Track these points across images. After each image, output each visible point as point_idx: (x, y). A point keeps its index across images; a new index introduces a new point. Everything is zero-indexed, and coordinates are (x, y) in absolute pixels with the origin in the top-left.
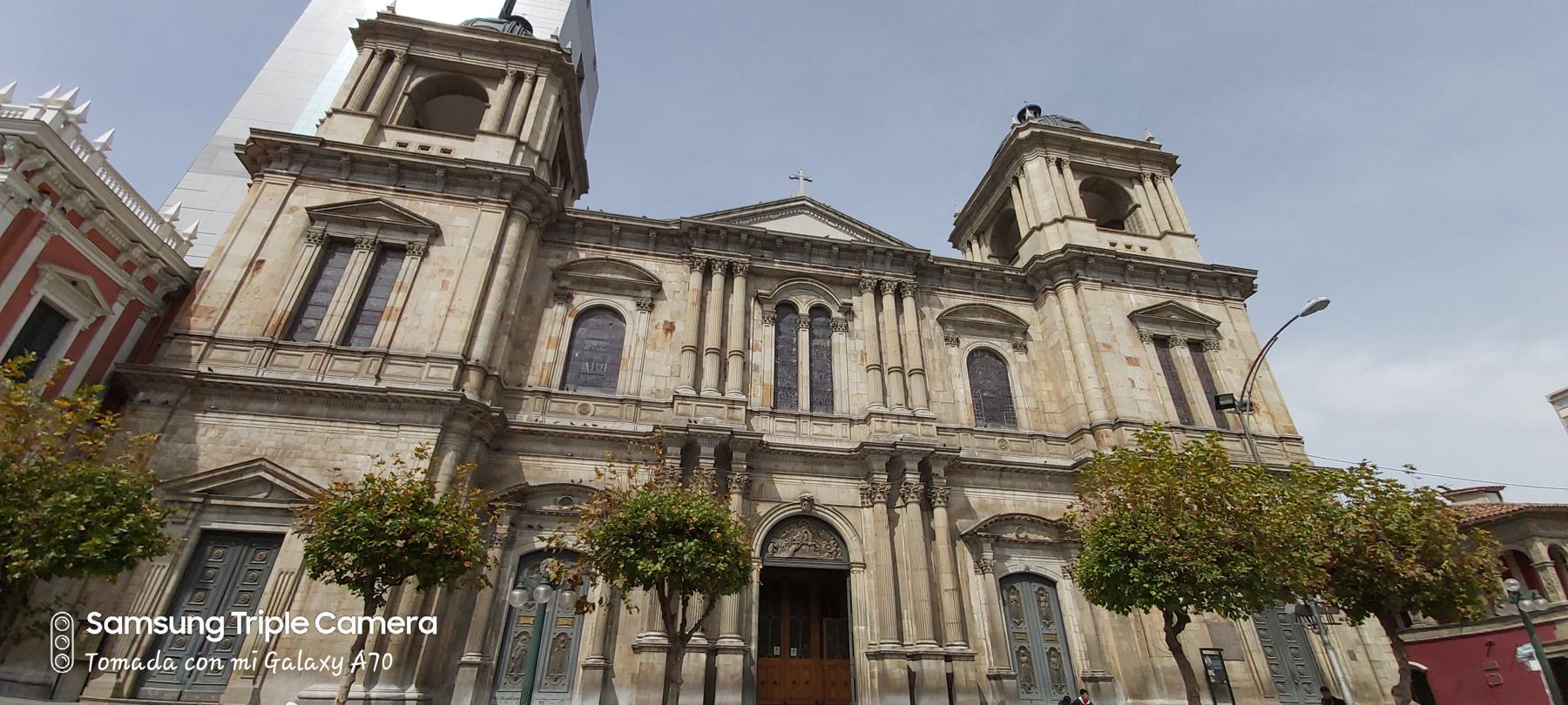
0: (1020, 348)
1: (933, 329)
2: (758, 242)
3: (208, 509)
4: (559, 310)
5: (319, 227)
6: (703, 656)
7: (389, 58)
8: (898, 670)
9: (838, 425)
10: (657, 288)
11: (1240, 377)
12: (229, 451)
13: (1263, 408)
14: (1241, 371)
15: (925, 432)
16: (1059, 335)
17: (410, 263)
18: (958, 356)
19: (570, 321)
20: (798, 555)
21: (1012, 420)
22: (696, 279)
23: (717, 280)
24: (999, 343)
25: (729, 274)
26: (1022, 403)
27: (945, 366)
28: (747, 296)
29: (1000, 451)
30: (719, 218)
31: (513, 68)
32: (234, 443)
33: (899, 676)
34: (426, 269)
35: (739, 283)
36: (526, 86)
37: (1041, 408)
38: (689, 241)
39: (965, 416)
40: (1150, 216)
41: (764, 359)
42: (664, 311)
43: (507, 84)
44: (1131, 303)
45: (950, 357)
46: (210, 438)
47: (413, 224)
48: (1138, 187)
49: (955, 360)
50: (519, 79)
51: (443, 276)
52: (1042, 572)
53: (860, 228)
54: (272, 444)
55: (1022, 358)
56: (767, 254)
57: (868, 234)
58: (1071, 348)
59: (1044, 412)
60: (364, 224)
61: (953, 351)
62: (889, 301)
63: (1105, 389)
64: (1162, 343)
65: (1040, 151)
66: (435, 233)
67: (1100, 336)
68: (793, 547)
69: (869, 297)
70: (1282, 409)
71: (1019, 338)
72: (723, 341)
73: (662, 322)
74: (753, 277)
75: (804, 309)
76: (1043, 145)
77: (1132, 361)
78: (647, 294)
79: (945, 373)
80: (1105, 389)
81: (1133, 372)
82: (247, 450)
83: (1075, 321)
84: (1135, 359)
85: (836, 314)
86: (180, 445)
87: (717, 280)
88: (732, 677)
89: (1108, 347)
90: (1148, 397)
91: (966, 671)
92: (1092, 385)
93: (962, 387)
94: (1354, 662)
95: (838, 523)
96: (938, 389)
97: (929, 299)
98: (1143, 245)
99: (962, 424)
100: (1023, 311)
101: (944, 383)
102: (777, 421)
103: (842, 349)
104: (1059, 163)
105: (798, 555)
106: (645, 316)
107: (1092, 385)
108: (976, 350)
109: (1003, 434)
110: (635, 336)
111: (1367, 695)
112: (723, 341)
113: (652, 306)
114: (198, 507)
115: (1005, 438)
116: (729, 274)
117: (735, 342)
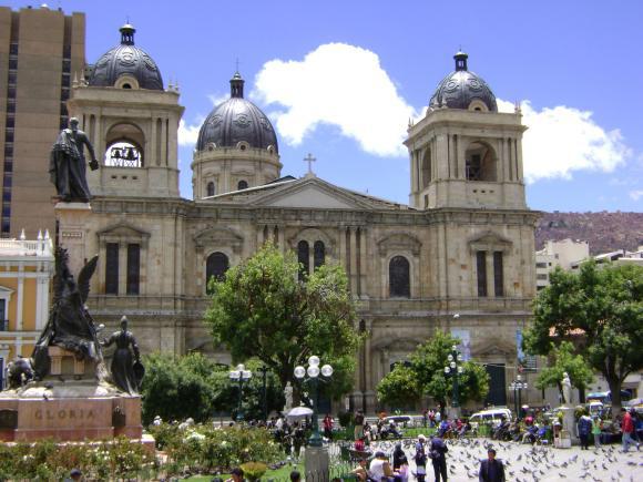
0: (417, 254)
4: (200, 257)
5: (102, 238)
10: (240, 239)
16: (433, 252)
17: (143, 253)
18: (385, 262)
19: (205, 263)
21: (408, 294)
22: (260, 236)
23: (271, 236)
25: (276, 230)
26: (413, 284)
31: (155, 117)
34: (150, 255)
35: (281, 237)
39: (385, 292)
45: (380, 263)
47: (140, 233)
50: (159, 120)
51: (157, 258)
55: (417, 261)
56: (293, 217)
58: (438, 258)
60: (119, 235)
61: (383, 260)
62: (353, 238)
63: (447, 282)
64: (481, 256)
65: (445, 130)
66: (149, 235)
67: (451, 255)
69: (343, 236)
71: (417, 249)
75: (311, 245)
76: (447, 126)
77: (464, 267)
78: (238, 244)
80: (447, 282)
81: (464, 274)
83: (441, 245)
85: (328, 245)
89: (453, 260)
92: (443, 279)
93: (385, 279)
106: (238, 258)
107: (443, 279)
116: (276, 230)
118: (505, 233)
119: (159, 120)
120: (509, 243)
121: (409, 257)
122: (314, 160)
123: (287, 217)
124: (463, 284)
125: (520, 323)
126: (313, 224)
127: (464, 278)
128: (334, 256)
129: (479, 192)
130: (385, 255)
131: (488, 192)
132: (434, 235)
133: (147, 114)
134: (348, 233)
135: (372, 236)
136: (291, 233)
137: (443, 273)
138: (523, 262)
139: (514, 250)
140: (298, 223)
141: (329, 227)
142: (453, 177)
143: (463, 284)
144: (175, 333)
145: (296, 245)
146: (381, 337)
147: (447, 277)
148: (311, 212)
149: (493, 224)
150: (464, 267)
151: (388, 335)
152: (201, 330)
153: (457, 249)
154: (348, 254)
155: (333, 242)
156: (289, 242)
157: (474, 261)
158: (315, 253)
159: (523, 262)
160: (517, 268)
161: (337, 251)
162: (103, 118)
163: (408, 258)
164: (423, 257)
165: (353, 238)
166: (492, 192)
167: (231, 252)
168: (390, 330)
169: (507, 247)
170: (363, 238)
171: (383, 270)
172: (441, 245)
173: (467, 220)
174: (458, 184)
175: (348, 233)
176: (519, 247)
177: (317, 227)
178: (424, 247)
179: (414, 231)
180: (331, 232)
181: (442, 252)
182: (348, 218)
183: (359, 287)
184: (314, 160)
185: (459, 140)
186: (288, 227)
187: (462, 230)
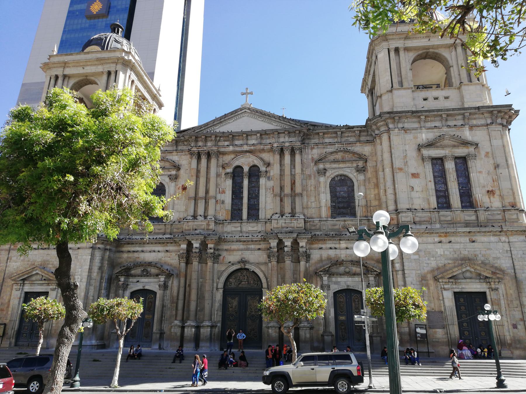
1: (312, 169)
2: (221, 138)
3: (25, 285)
6: (194, 329)
7: (57, 77)
8: (274, 334)
9: (260, 225)
10: (178, 168)
11: (487, 175)
12: (28, 264)
13: (497, 193)
14: (489, 171)
15: (298, 226)
18: (324, 182)
20: (240, 286)
22: (194, 162)
23: (204, 161)
24: (349, 171)
25: (209, 155)
27: (317, 188)
28: (217, 166)
29: (342, 230)
30: (204, 128)
32: (29, 261)
33: (274, 336)
35: (213, 161)
36: (113, 77)
37: (369, 204)
38: (190, 143)
39: (325, 212)
40: (456, 73)
41: (228, 197)
42: (181, 182)
43: (105, 77)
44: (423, 140)
45: (320, 183)
46: (22, 260)
48: (454, 53)
49: (322, 185)
50: (109, 73)
52: (356, 289)
53: (274, 119)
54: (40, 260)
55: (361, 177)
56: (226, 143)
57: (278, 122)
58: (383, 170)
59: (371, 206)
61: (322, 179)
62: (287, 158)
63: (395, 194)
65: (385, 44)
67: (398, 164)
68: (239, 282)
69: (277, 157)
70: (511, 191)
72: (207, 192)
73: (181, 186)
74: (221, 156)
75: (246, 169)
76: (387, 40)
77: (415, 176)
78: (174, 172)
79: (317, 192)
80: (395, 194)
81: (415, 182)
82: (33, 263)
84: (417, 174)
85: (263, 169)
86: (14, 263)
87: (204, 161)
88: (206, 337)
89: (400, 169)
90: (420, 196)
91: (305, 334)
92: (390, 191)
93: (325, 198)
94: (515, 329)
95: (257, 271)
96: (312, 201)
97: (312, 151)
98: (446, 95)
99: (323, 218)
100: (366, 150)
101: (315, 197)
102: (232, 226)
103: (264, 187)
104: (397, 50)
105: (240, 286)
106: (173, 184)
108: (337, 176)
109: (345, 221)
110: (169, 195)
111: (518, 346)
112: (207, 192)
113: (176, 178)
114: (22, 285)
115: (346, 223)
116: (209, 155)
117: (212, 193)
118: (467, 134)
119: (109, 73)
120: (476, 145)
121: (352, 174)
122: (251, 93)
123: (220, 144)
124: (414, 194)
125: (503, 238)
126: (246, 148)
127: (416, 188)
128: (269, 178)
129: (431, 99)
130: (325, 173)
131: (441, 98)
132: (379, 147)
133: (100, 69)
134: (282, 151)
135: (310, 157)
136: (227, 158)
137: (389, 183)
138: (497, 167)
139: (483, 153)
140: (231, 148)
141: (263, 150)
142: (396, 85)
143: (414, 194)
144: (93, 255)
145: (230, 170)
146: (321, 260)
147: (395, 189)
148: (248, 134)
149: (449, 126)
150: (415, 176)
151: (329, 258)
152: (130, 255)
153: (406, 156)
154: (282, 175)
155: (268, 165)
156: (223, 168)
157: (428, 170)
158: (250, 177)
159: (497, 167)
160: (489, 173)
161: (272, 174)
162: (65, 76)
163: (351, 176)
164: (369, 174)
165: (287, 158)
166: (447, 98)
167: (167, 179)
168: (332, 253)
169: (471, 150)
170: (298, 157)
171: (322, 189)
172: (386, 156)
173: (416, 125)
174: (402, 92)
175: (282, 151)
176: (489, 150)
177: (250, 152)
178: (370, 164)
179: (358, 148)
180: (266, 156)
181: (387, 162)
182: (282, 140)
183: (293, 209)
184: (251, 93)
185: (402, 53)
186: (224, 153)
187: (409, 137)
